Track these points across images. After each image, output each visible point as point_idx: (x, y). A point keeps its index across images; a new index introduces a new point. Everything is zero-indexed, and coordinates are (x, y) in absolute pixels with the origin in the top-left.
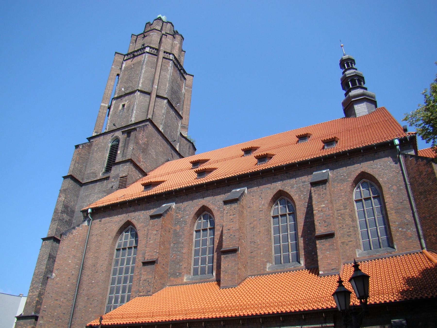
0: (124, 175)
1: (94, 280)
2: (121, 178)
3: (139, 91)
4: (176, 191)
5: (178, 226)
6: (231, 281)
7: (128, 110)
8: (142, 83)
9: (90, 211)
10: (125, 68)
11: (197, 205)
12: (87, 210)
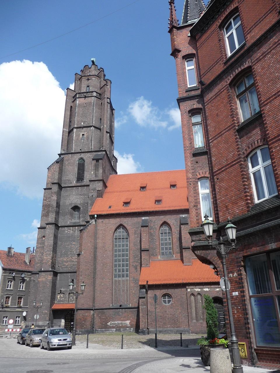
0: (100, 189)
1: (105, 255)
2: (98, 191)
3: (94, 126)
4: (150, 212)
5: (152, 230)
6: (188, 262)
7: (88, 140)
8: (95, 121)
9: (96, 216)
10: (79, 104)
11: (162, 220)
12: (94, 215)
